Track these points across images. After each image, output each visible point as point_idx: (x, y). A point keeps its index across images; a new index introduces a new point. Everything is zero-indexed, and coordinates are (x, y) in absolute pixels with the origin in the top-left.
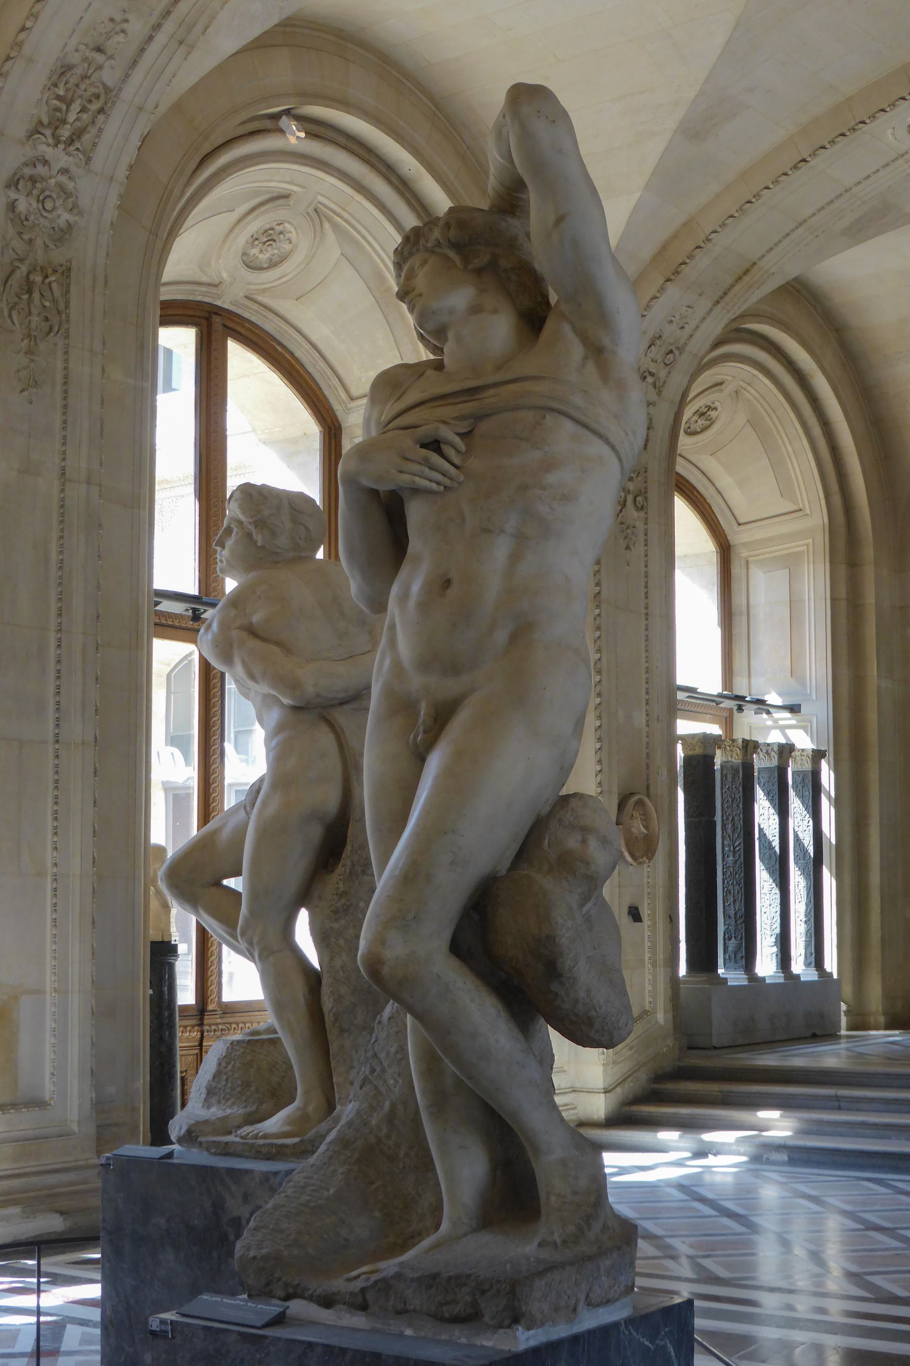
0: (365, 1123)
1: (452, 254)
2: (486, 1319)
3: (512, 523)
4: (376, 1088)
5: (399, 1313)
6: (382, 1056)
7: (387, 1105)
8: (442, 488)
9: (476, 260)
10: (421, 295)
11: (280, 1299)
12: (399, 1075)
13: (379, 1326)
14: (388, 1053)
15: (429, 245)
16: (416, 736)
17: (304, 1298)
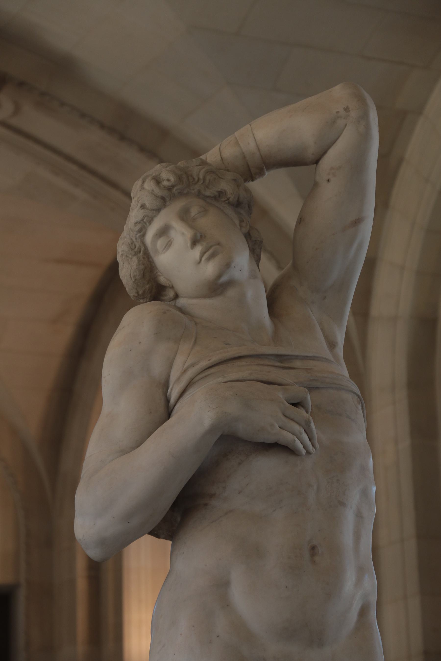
1: (229, 210)
3: (354, 498)
8: (305, 451)
9: (244, 224)
10: (219, 244)
15: (208, 193)
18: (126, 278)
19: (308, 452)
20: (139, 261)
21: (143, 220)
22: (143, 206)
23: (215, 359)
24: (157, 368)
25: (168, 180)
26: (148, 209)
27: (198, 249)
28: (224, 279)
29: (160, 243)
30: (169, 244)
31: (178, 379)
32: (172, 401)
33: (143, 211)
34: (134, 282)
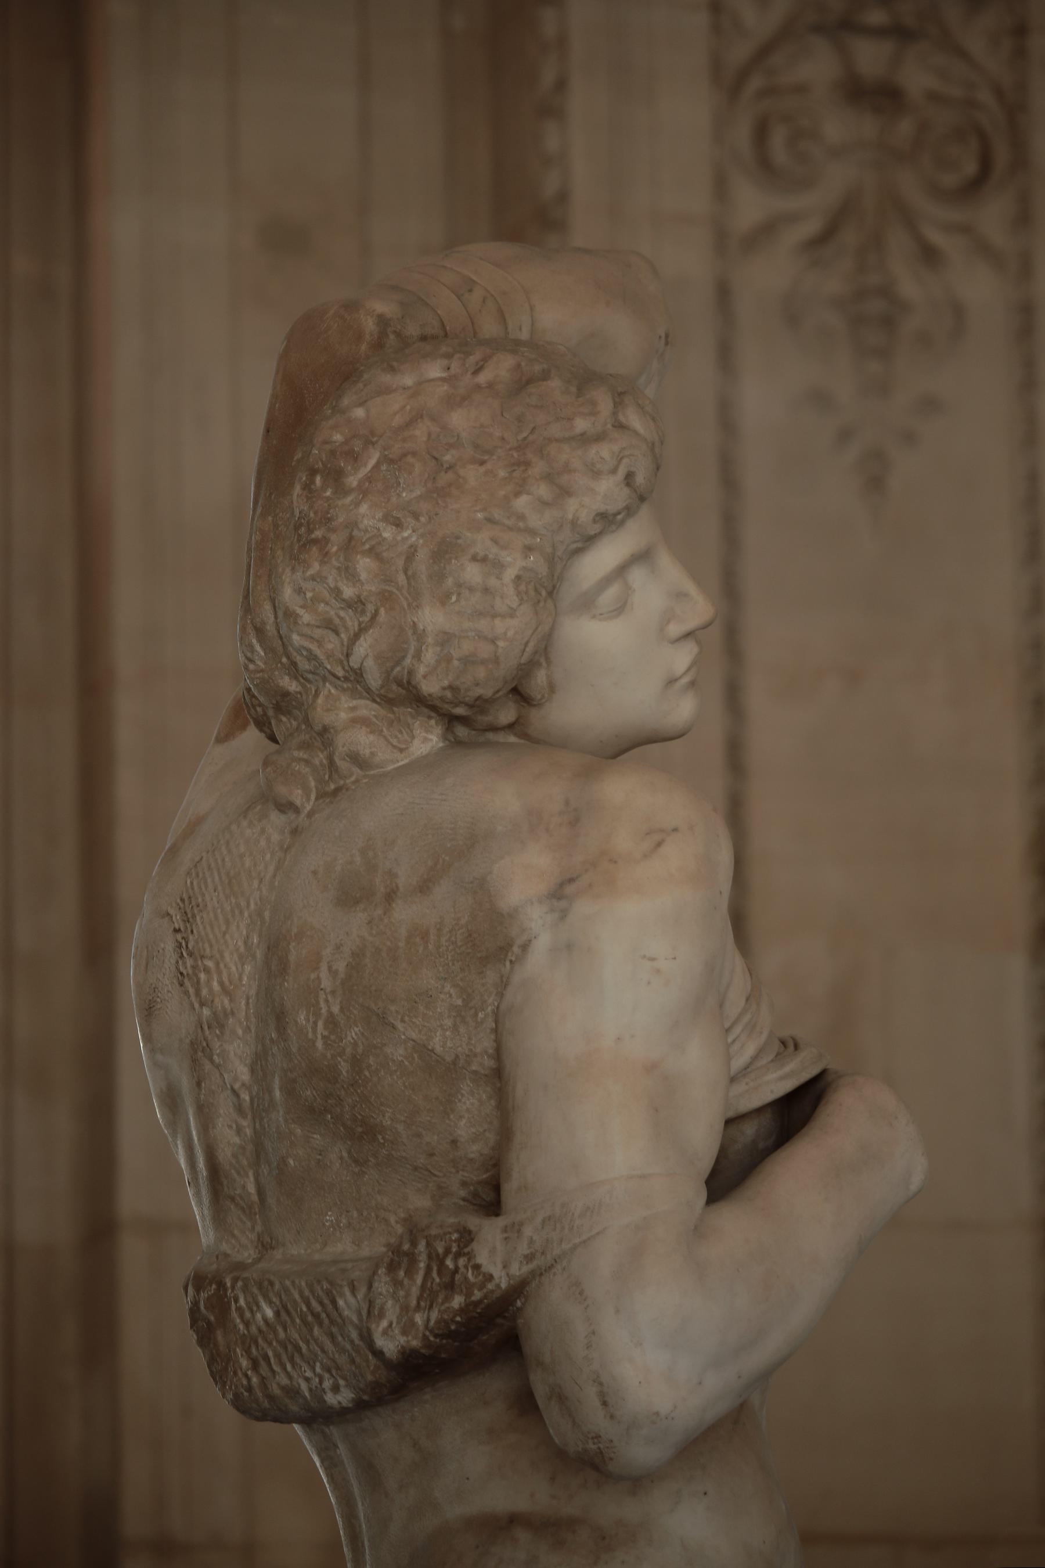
18: (501, 644)
26: (635, 491)
33: (626, 491)
34: (520, 664)
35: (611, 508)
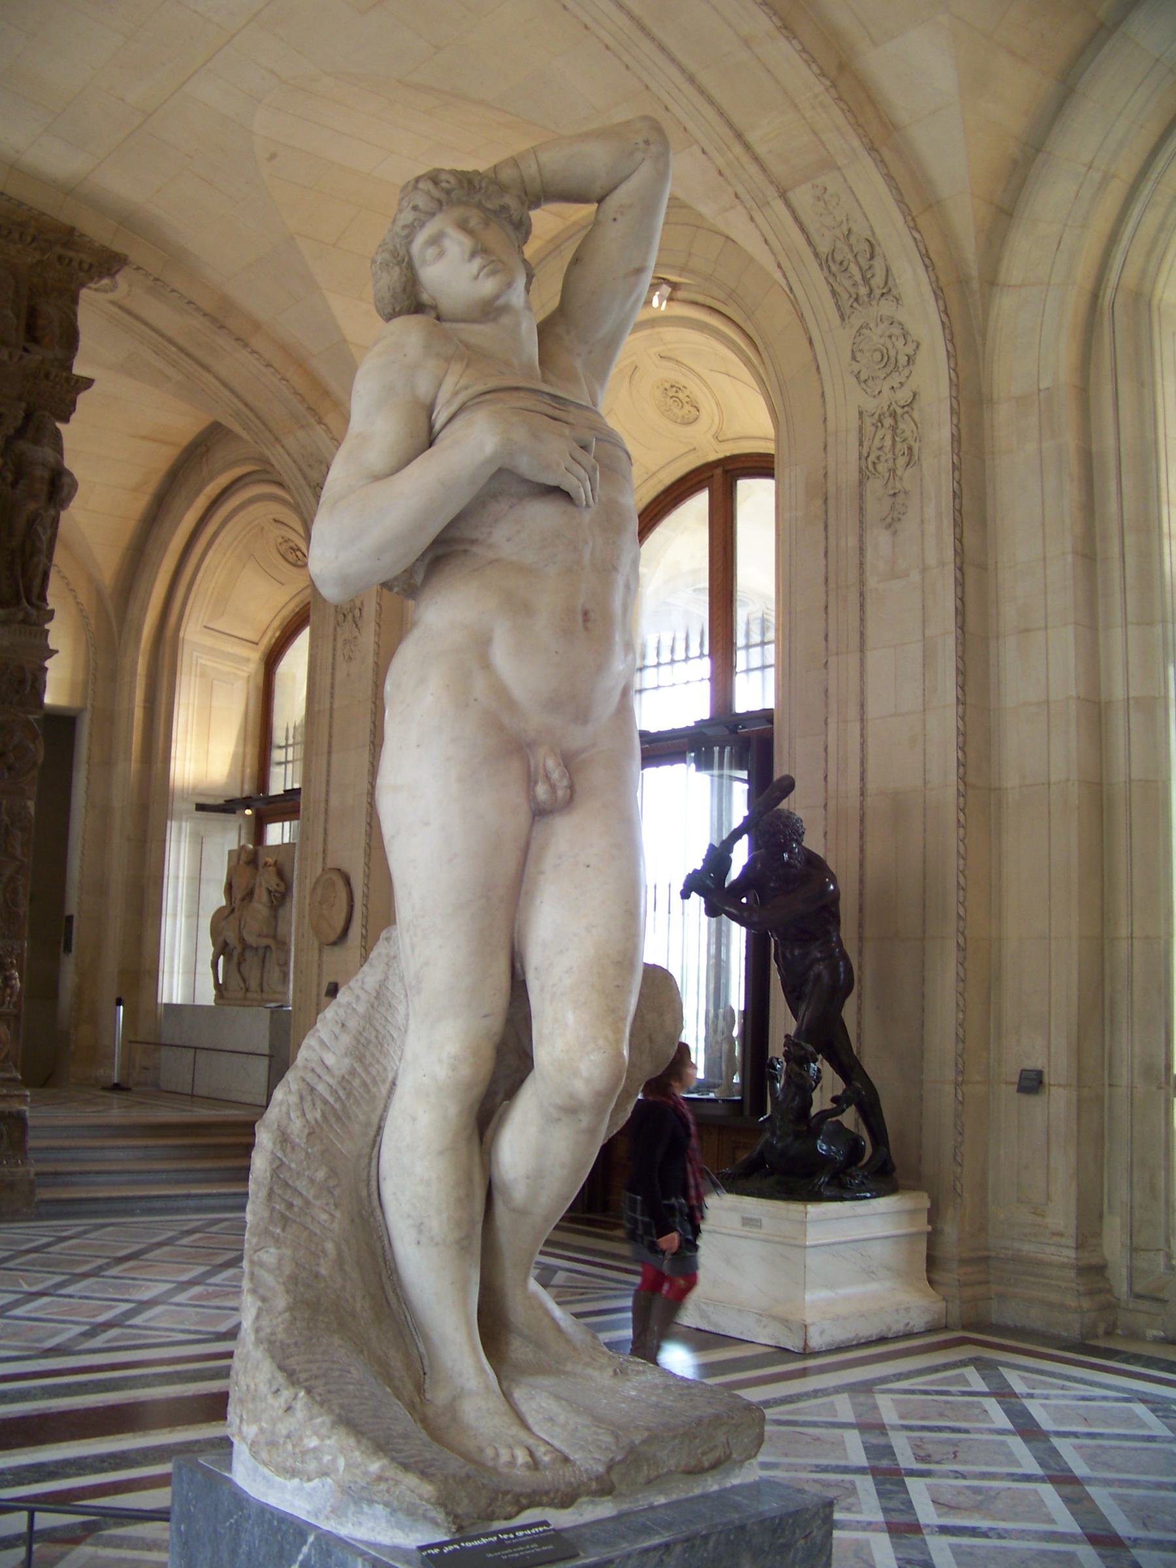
0: (317, 1276)
2: (734, 1456)
4: (306, 1228)
5: (649, 1482)
6: (301, 1185)
7: (330, 1246)
11: (508, 1517)
12: (336, 1206)
13: (625, 1507)
14: (312, 1181)
15: (489, 206)
16: (553, 788)
17: (540, 1504)
19: (588, 505)
20: (401, 269)
21: (412, 223)
22: (415, 208)
23: (492, 383)
24: (424, 388)
25: (448, 182)
27: (477, 262)
28: (501, 302)
29: (431, 252)
30: (441, 254)
31: (449, 402)
32: (437, 426)
33: (413, 213)
35: (408, 222)
